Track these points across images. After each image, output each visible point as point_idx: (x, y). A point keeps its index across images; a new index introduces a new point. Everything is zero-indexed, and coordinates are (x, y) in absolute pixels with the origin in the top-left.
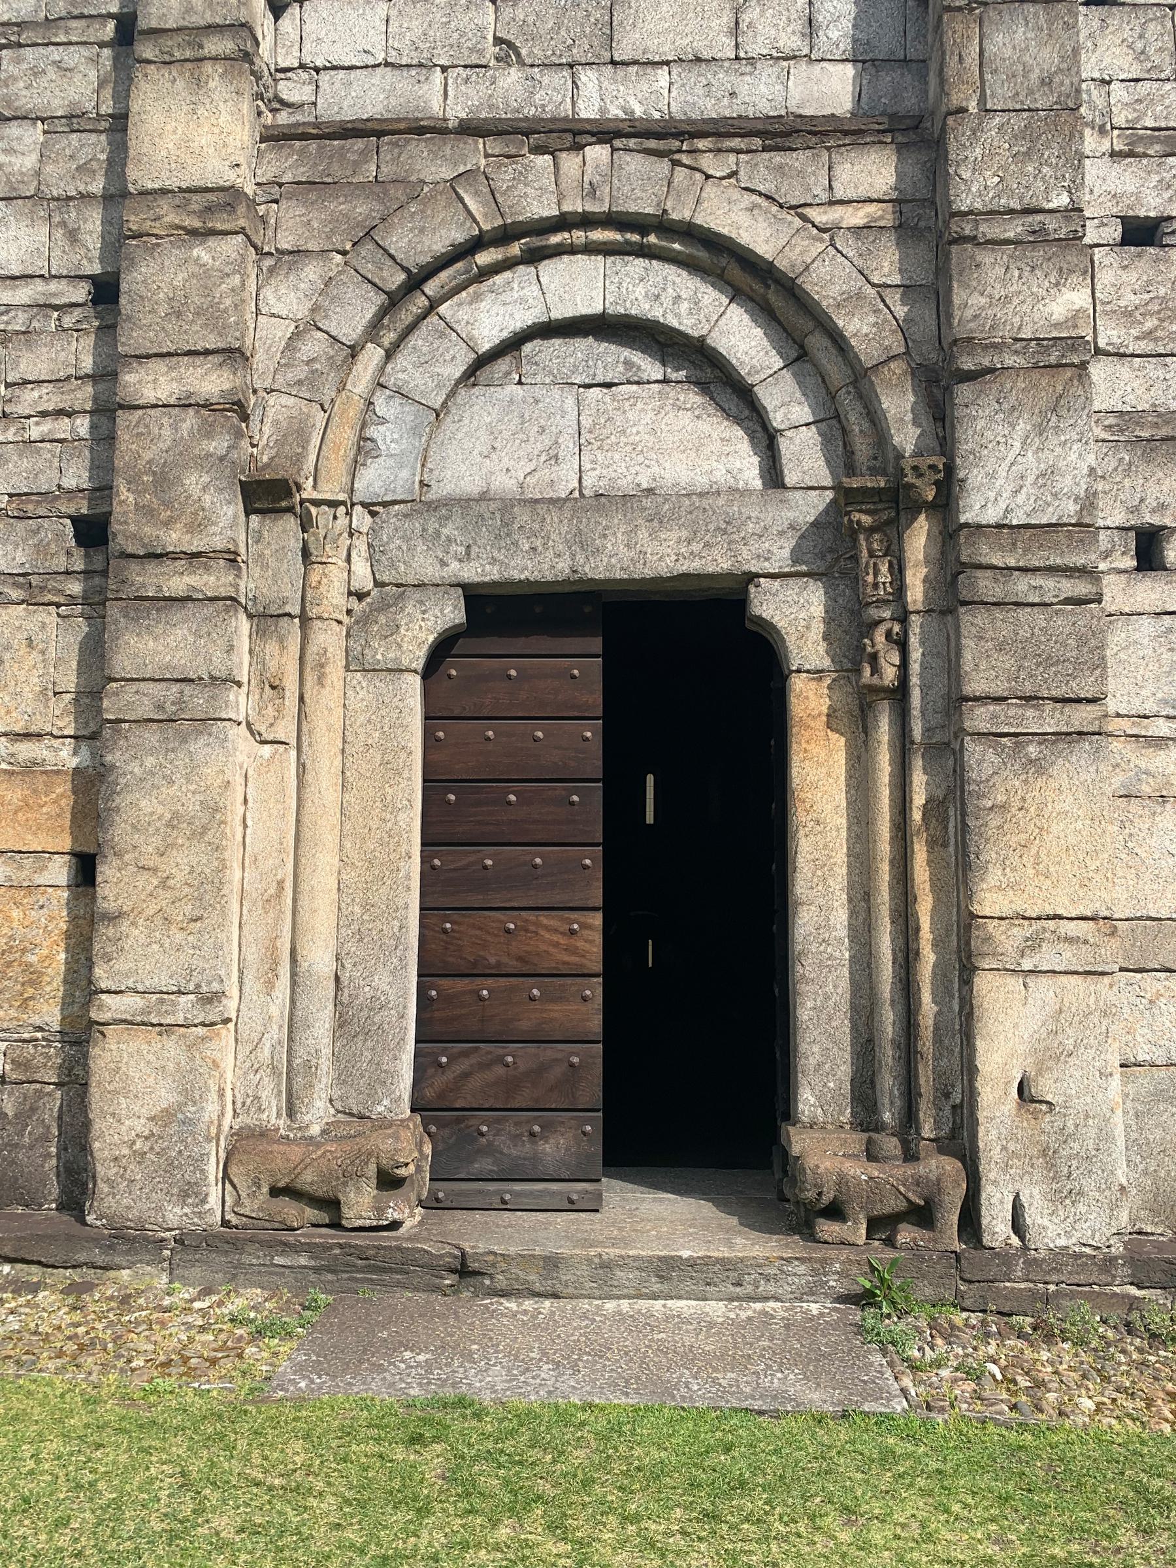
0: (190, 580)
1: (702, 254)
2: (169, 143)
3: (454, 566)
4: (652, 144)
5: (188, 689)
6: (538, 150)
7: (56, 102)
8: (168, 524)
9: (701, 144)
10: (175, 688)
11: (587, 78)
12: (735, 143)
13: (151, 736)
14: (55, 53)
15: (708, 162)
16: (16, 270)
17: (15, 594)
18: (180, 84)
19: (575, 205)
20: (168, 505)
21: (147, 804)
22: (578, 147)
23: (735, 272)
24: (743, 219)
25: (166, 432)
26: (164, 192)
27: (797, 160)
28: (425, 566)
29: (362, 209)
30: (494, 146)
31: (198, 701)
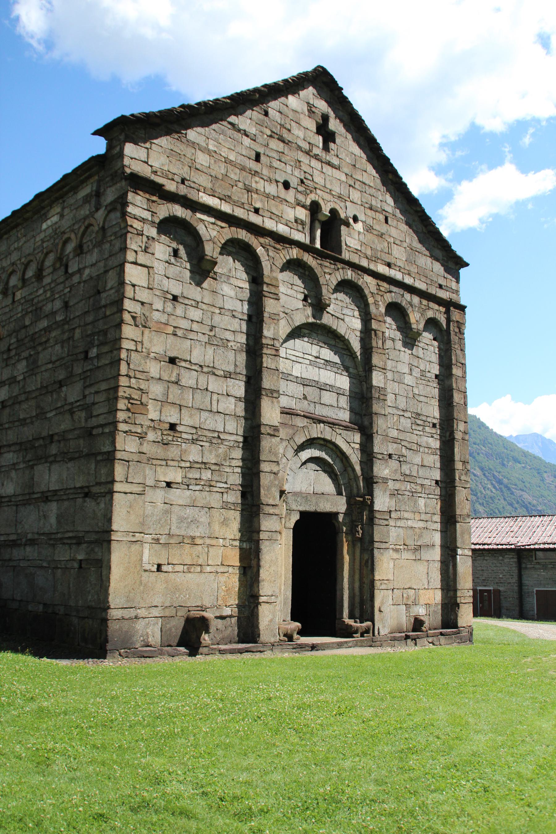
0: (273, 510)
1: (334, 448)
2: (268, 415)
3: (299, 507)
4: (330, 425)
5: (273, 533)
6: (314, 423)
7: (238, 394)
8: (270, 498)
9: (337, 427)
10: (271, 533)
11: (317, 406)
12: (341, 428)
13: (267, 543)
14: (237, 382)
15: (337, 430)
16: (231, 432)
17: (233, 508)
18: (270, 402)
19: (319, 436)
20: (269, 494)
21: (267, 557)
22: (319, 423)
23: (339, 453)
24: (342, 443)
25: (269, 478)
26: (267, 425)
27: (349, 433)
28: (294, 507)
29: (291, 432)
30: (308, 420)
31: (275, 536)
